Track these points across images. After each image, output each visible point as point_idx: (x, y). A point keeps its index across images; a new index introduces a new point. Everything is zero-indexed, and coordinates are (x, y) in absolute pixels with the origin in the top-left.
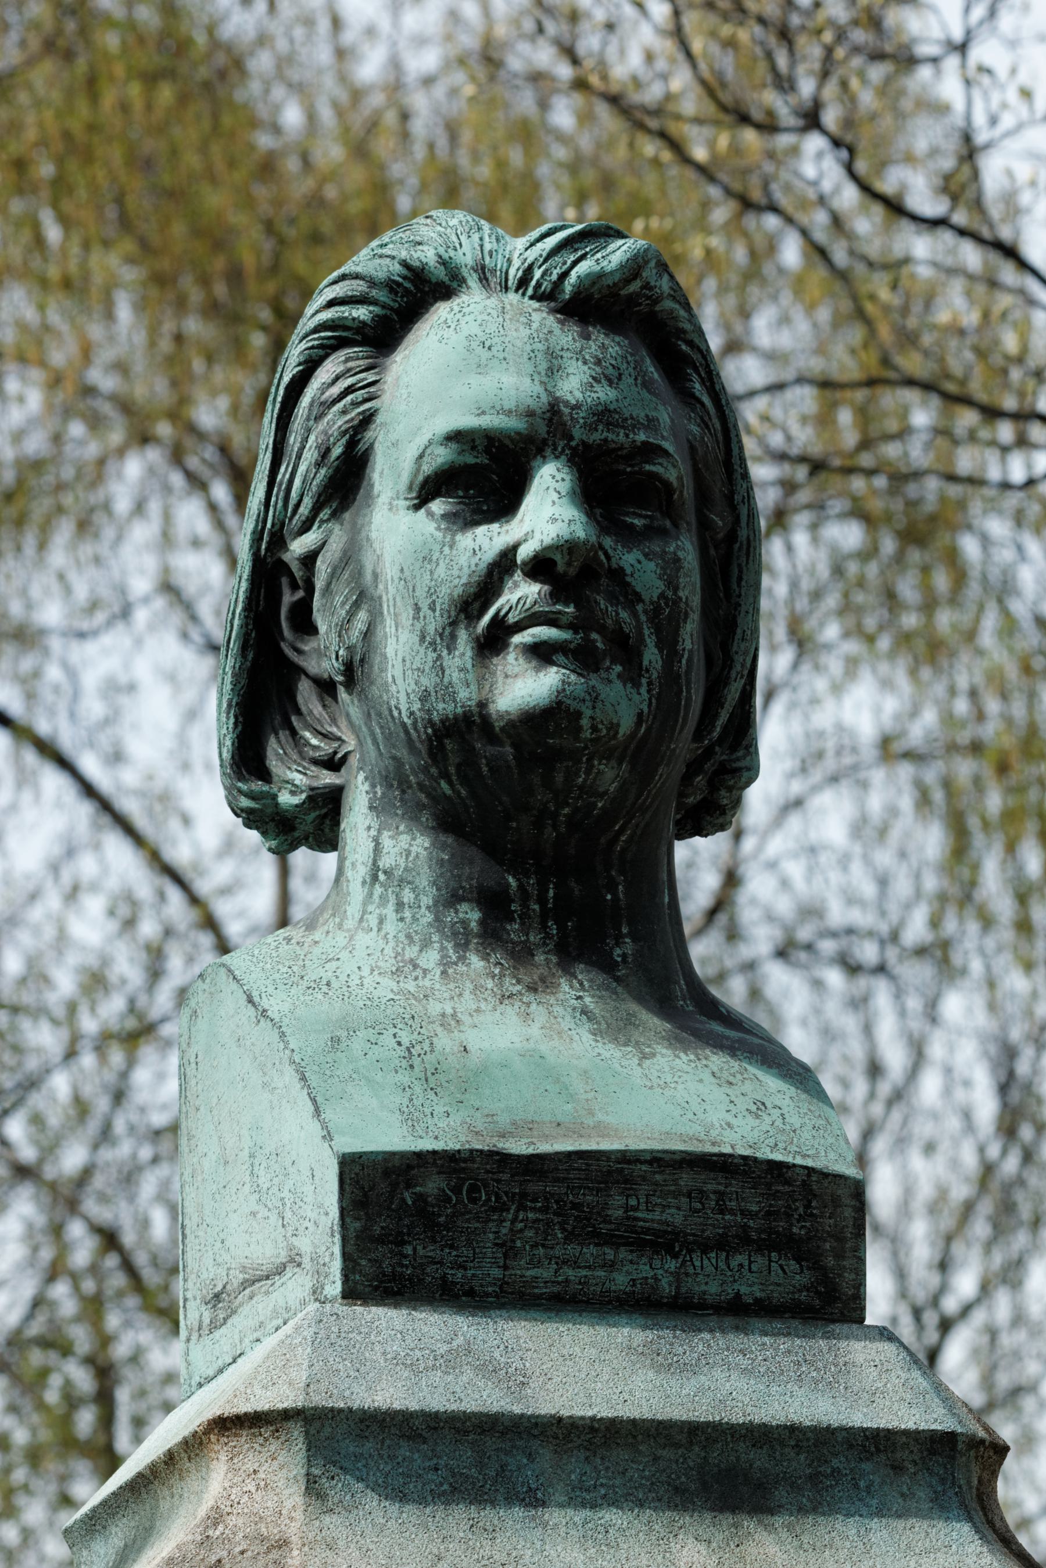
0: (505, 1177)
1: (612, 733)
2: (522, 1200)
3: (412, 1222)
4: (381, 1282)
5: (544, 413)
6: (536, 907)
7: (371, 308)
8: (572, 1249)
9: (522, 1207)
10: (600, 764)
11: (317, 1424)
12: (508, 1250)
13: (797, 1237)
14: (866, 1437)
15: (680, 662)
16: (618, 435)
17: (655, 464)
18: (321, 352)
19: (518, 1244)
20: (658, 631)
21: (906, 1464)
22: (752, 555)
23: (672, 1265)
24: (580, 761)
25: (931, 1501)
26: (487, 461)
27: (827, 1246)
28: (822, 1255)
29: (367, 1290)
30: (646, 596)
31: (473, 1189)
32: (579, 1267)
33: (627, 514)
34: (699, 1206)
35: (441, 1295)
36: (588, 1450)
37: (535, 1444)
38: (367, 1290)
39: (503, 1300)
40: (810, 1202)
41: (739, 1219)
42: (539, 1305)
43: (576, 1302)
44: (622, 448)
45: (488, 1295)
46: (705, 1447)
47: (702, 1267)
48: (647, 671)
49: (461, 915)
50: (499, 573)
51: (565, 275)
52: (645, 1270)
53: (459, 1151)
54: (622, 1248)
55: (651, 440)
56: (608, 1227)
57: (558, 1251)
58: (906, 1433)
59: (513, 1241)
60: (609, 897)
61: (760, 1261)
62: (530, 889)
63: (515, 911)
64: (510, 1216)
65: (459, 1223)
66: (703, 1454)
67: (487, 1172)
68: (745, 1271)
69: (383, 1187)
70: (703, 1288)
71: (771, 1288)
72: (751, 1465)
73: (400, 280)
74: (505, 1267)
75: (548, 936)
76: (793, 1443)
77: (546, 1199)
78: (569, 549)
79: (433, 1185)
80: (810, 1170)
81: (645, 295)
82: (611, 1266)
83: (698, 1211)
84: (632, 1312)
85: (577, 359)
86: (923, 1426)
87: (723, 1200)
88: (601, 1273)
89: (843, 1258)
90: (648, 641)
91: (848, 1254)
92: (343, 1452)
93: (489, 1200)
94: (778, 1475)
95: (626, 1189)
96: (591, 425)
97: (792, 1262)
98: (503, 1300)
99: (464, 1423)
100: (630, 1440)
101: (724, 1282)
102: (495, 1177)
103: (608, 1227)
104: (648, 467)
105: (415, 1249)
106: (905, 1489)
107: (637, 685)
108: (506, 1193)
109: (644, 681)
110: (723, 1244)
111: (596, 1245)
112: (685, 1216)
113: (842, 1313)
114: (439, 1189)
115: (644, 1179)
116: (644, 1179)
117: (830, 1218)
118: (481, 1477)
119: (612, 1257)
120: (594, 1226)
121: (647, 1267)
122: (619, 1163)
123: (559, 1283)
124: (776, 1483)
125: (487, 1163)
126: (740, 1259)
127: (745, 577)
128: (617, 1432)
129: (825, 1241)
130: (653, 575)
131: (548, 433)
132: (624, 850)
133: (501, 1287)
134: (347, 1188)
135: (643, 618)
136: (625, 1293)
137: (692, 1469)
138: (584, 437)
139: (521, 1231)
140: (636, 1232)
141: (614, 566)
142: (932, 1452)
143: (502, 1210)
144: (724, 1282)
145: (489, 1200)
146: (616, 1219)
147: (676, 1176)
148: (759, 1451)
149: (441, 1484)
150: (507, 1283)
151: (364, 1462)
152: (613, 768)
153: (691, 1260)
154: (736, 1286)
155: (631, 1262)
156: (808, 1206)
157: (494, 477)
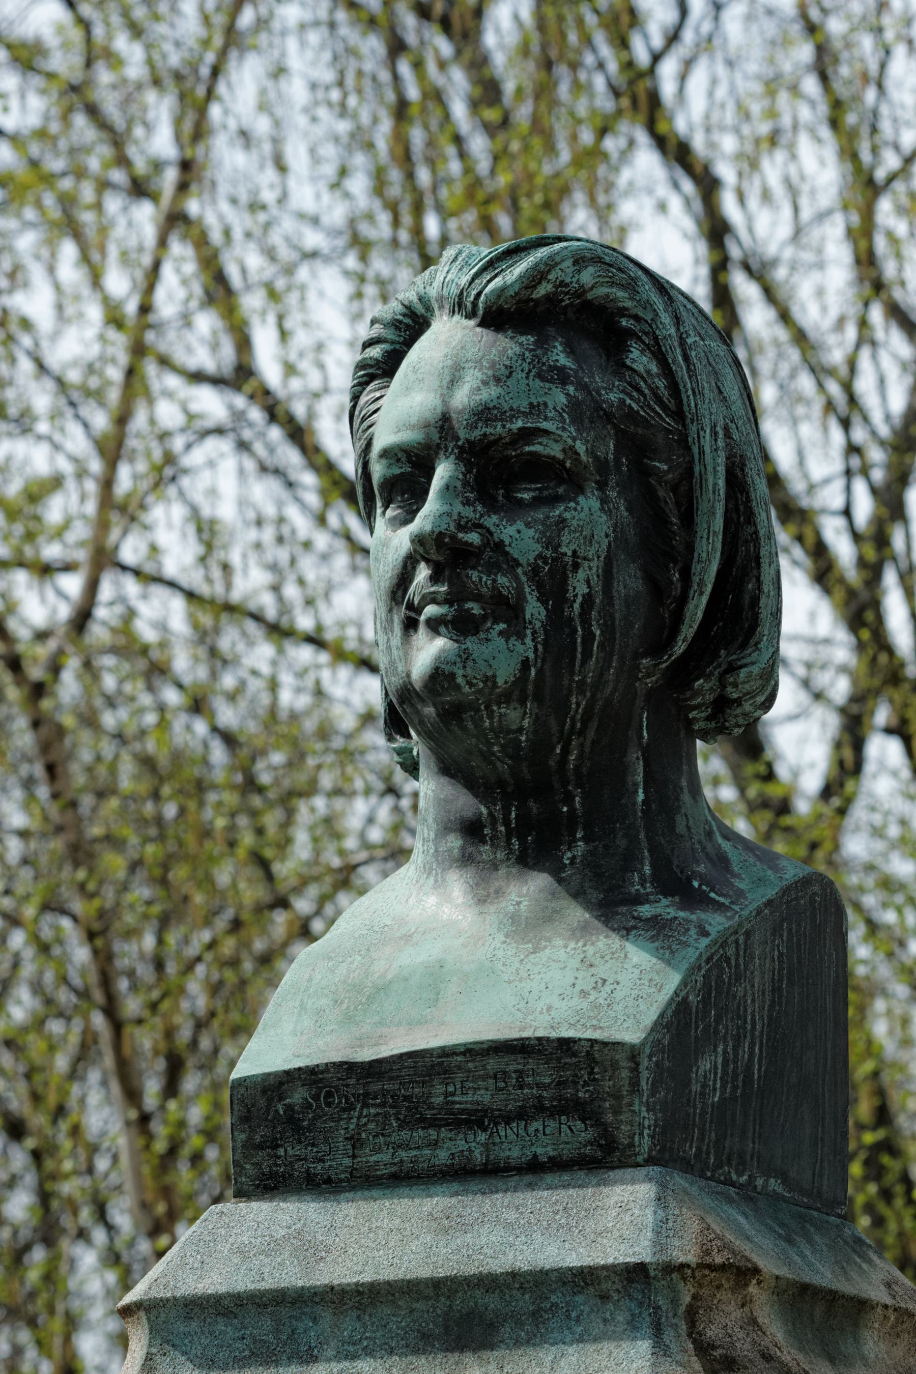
0: (352, 1081)
1: (490, 684)
2: (365, 1099)
3: (283, 1129)
4: (262, 1181)
5: (437, 422)
6: (503, 829)
7: (383, 346)
8: (405, 1134)
9: (366, 1105)
10: (499, 708)
11: (154, 1312)
12: (355, 1142)
13: (582, 1101)
14: (575, 1275)
15: (572, 607)
16: (496, 427)
17: (534, 444)
18: (359, 388)
19: (364, 1135)
20: (540, 586)
21: (611, 1293)
22: (704, 486)
23: (482, 1137)
24: (478, 710)
25: (628, 1323)
26: (410, 469)
27: (607, 1104)
28: (603, 1113)
29: (251, 1188)
30: (523, 561)
31: (329, 1095)
32: (410, 1149)
33: (519, 491)
34: (502, 1085)
35: (307, 1185)
36: (360, 1309)
37: (318, 1310)
38: (251, 1188)
39: (353, 1183)
40: (593, 1069)
41: (535, 1091)
42: (380, 1184)
43: (410, 1178)
44: (501, 438)
45: (341, 1181)
46: (449, 1297)
47: (506, 1136)
48: (530, 623)
49: (449, 844)
50: (412, 563)
51: (479, 295)
52: (461, 1145)
53: (317, 1066)
54: (443, 1129)
55: (529, 425)
56: (432, 1112)
57: (394, 1138)
58: (605, 1267)
59: (359, 1134)
60: (565, 809)
61: (552, 1124)
62: (496, 814)
63: (487, 835)
64: (356, 1114)
65: (318, 1125)
66: (448, 1303)
67: (339, 1079)
68: (540, 1135)
69: (262, 1103)
70: (508, 1153)
71: (561, 1146)
72: (486, 1308)
73: (400, 317)
74: (354, 1156)
75: (511, 852)
76: (517, 1286)
77: (384, 1095)
78: (419, 541)
79: (298, 1096)
80: (593, 1042)
81: (562, 292)
82: (435, 1144)
83: (502, 1089)
84: (452, 1181)
85: (475, 367)
86: (621, 1260)
87: (522, 1077)
88: (427, 1152)
89: (620, 1113)
90: (529, 597)
91: (625, 1109)
92: (175, 1332)
93: (340, 1102)
94: (507, 1314)
95: (445, 1078)
96: (471, 425)
97: (579, 1122)
98: (353, 1183)
99: (261, 1298)
100: (391, 1298)
101: (524, 1147)
102: (344, 1083)
103: (432, 1112)
104: (527, 449)
105: (286, 1151)
106: (608, 1316)
107: (521, 637)
108: (353, 1095)
109: (528, 632)
110: (522, 1115)
111: (423, 1128)
112: (492, 1095)
113: (620, 1161)
114: (303, 1098)
115: (459, 1068)
116: (459, 1068)
117: (609, 1080)
118: (275, 1341)
119: (435, 1137)
120: (421, 1114)
121: (463, 1142)
122: (440, 1057)
123: (395, 1164)
124: (504, 1321)
125: (338, 1072)
126: (536, 1125)
127: (700, 507)
128: (378, 1293)
129: (606, 1100)
130: (531, 541)
131: (440, 438)
132: (577, 768)
133: (351, 1173)
134: (235, 1106)
135: (524, 579)
136: (446, 1166)
137: (439, 1316)
138: (467, 436)
139: (365, 1124)
140: (454, 1114)
141: (497, 540)
142: (630, 1281)
143: (350, 1110)
144: (524, 1147)
145: (340, 1102)
146: (438, 1104)
147: (485, 1062)
148: (492, 1296)
149: (244, 1350)
150: (356, 1169)
151: (190, 1338)
152: (515, 709)
153: (497, 1131)
154: (533, 1149)
155: (450, 1139)
156: (591, 1073)
157: (422, 479)
